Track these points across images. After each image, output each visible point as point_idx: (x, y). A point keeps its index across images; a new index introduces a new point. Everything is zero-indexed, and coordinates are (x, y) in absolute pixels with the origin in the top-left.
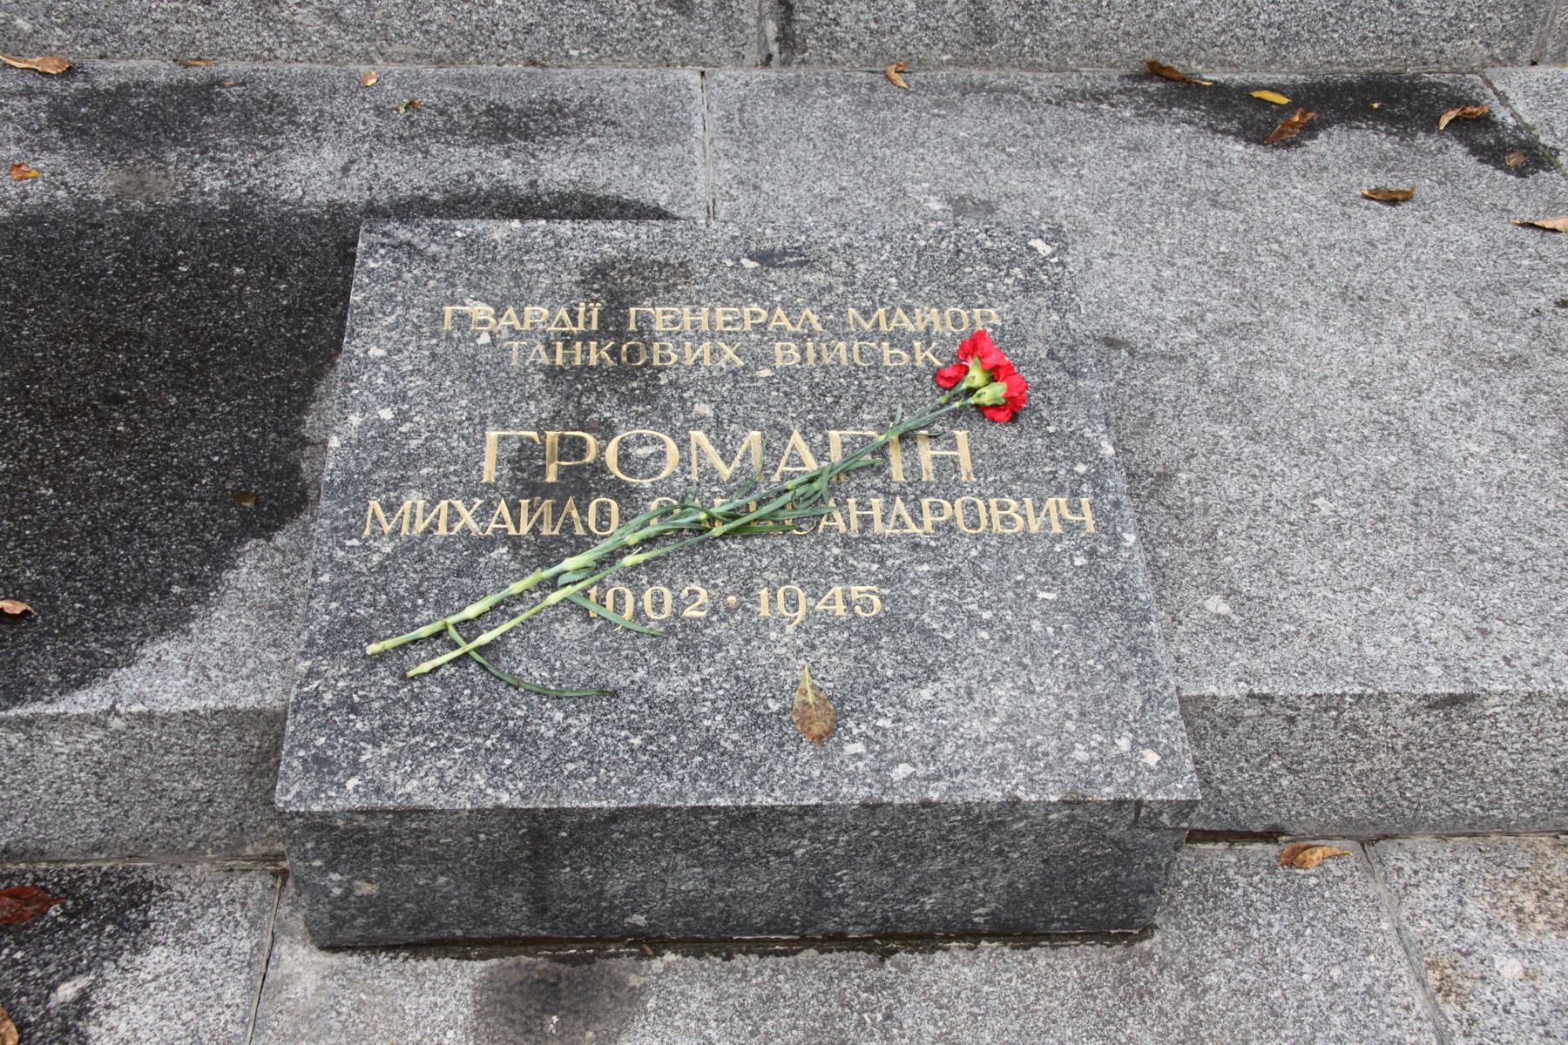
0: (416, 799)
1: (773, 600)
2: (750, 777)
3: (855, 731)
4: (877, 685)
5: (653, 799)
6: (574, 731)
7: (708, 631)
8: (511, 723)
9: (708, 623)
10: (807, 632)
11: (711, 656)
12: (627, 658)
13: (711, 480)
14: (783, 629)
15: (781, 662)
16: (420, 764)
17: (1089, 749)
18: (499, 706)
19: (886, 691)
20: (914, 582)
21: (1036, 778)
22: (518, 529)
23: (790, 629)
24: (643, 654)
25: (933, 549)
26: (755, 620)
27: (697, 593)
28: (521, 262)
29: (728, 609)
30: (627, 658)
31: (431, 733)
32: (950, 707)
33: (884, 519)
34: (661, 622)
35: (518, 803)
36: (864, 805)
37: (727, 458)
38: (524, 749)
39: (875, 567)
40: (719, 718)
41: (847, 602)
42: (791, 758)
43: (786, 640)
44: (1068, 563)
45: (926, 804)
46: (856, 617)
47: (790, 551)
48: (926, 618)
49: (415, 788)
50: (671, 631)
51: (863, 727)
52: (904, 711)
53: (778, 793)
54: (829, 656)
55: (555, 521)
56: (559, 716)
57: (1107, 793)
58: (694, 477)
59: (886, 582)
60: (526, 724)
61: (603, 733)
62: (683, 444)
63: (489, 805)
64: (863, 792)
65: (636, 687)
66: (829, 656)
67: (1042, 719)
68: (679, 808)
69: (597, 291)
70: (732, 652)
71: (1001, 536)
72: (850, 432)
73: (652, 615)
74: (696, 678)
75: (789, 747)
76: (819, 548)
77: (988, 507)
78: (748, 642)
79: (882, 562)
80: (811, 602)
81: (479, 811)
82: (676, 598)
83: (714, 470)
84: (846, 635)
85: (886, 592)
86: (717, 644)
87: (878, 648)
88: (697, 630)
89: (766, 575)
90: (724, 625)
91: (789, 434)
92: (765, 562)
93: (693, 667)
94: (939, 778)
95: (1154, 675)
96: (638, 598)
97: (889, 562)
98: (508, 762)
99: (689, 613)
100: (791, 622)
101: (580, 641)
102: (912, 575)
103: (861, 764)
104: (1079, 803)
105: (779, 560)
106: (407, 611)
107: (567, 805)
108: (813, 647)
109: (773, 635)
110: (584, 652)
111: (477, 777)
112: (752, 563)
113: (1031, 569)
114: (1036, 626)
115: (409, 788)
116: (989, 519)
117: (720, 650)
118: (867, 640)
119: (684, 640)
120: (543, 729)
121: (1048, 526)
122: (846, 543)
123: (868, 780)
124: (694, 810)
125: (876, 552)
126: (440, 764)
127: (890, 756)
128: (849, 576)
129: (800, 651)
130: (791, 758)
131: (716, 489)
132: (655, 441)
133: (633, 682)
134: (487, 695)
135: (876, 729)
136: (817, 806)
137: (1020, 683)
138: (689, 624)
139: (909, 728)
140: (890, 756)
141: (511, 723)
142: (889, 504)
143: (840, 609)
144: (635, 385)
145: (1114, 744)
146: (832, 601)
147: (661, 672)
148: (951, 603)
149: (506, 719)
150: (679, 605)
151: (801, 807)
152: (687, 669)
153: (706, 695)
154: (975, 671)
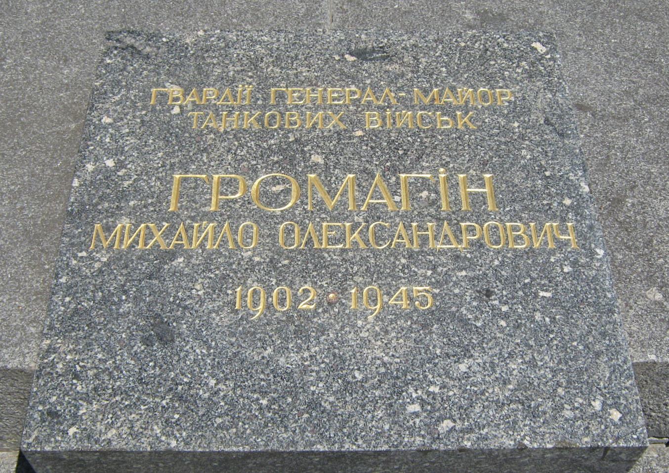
0: (114, 443)
1: (359, 298)
2: (341, 430)
3: (414, 395)
4: (430, 361)
5: (274, 446)
6: (222, 394)
7: (315, 320)
8: (180, 387)
9: (316, 313)
10: (382, 320)
11: (318, 338)
12: (260, 339)
13: (321, 209)
14: (366, 318)
15: (365, 343)
16: (118, 418)
17: (574, 409)
18: (172, 375)
19: (436, 365)
20: (456, 284)
21: (537, 430)
22: (191, 244)
23: (371, 318)
24: (270, 337)
25: (469, 260)
26: (347, 311)
27: (309, 291)
28: (203, 58)
29: (330, 304)
30: (260, 339)
31: (126, 394)
32: (479, 377)
33: (436, 238)
34: (283, 313)
35: (182, 447)
36: (419, 451)
37: (331, 193)
38: (188, 408)
39: (429, 273)
40: (321, 385)
41: (411, 299)
42: (370, 415)
43: (368, 326)
45: (463, 450)
46: (416, 310)
47: (372, 261)
49: (114, 436)
50: (290, 319)
51: (420, 392)
52: (447, 380)
53: (360, 442)
54: (398, 339)
55: (215, 239)
56: (212, 382)
57: (586, 441)
58: (309, 207)
59: (438, 284)
60: (190, 388)
61: (241, 396)
62: (303, 184)
63: (163, 448)
64: (418, 440)
65: (265, 361)
66: (398, 339)
67: (542, 386)
68: (291, 452)
69: (251, 77)
70: (331, 335)
71: (515, 250)
72: (414, 175)
73: (278, 308)
74: (306, 354)
76: (392, 259)
77: (505, 229)
78: (342, 328)
79: (434, 269)
80: (386, 298)
81: (156, 452)
82: (295, 295)
84: (409, 323)
85: (437, 291)
86: (322, 329)
87: (431, 333)
88: (308, 319)
89: (355, 278)
90: (327, 315)
91: (373, 177)
92: (356, 268)
93: (304, 346)
94: (470, 430)
95: (617, 353)
97: (439, 269)
98: (177, 416)
99: (303, 306)
100: (372, 314)
101: (229, 327)
102: (454, 279)
103: (417, 421)
104: (566, 448)
105: (365, 267)
107: (215, 449)
108: (387, 332)
109: (360, 323)
110: (233, 334)
111: (155, 427)
112: (347, 270)
113: (534, 275)
114: (538, 316)
115: (109, 435)
117: (323, 334)
118: (424, 326)
119: (298, 328)
120: (201, 392)
121: (546, 243)
122: (411, 255)
123: (422, 432)
124: (302, 453)
125: (431, 262)
126: (130, 418)
127: (437, 414)
128: (412, 279)
129: (377, 334)
130: (370, 415)
131: (323, 216)
132: (284, 181)
133: (263, 358)
134: (165, 366)
135: (429, 394)
136: (387, 451)
137: (527, 359)
138: (302, 314)
139: (451, 393)
140: (437, 414)
141: (180, 387)
142: (440, 226)
143: (404, 304)
144: (272, 142)
145: (590, 405)
147: (282, 350)
149: (177, 384)
151: (375, 452)
152: (300, 348)
153: (313, 367)
154: (497, 350)
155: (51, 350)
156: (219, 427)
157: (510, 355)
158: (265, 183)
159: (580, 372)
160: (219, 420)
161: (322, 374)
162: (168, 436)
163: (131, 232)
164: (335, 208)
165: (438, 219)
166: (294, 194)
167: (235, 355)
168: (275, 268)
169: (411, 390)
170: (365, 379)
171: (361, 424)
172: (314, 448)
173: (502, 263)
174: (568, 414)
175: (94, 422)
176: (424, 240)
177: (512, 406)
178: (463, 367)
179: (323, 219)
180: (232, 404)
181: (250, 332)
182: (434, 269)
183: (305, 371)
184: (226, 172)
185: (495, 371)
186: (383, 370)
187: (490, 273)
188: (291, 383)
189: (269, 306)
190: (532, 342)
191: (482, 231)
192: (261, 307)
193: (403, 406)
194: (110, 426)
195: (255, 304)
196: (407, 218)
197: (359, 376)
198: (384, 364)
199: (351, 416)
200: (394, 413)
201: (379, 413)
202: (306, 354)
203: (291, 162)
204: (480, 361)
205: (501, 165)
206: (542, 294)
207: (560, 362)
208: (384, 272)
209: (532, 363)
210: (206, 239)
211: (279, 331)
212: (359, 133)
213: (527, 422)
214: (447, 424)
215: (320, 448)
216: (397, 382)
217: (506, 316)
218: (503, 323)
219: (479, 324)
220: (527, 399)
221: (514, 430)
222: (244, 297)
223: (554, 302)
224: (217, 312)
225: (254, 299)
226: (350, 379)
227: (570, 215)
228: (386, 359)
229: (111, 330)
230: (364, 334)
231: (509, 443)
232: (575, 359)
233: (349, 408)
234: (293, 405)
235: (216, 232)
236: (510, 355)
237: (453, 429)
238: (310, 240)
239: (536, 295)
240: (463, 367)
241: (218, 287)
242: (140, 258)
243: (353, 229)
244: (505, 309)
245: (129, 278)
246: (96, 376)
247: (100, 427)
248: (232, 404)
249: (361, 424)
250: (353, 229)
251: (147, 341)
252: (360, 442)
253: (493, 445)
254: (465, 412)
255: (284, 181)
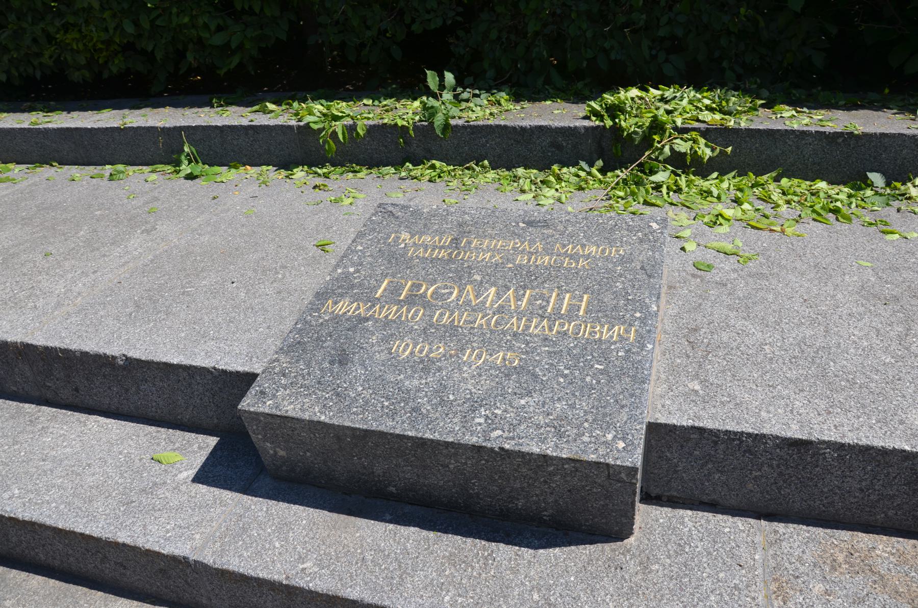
1: (470, 355)
5: (382, 428)
15: (464, 380)
20: (538, 354)
23: (474, 367)
29: (451, 355)
32: (532, 409)
33: (536, 327)
35: (327, 420)
37: (477, 297)
44: (615, 354)
46: (505, 365)
48: (537, 370)
49: (290, 409)
50: (422, 361)
59: (527, 353)
64: (475, 439)
75: (450, 416)
77: (586, 326)
80: (488, 357)
83: (471, 301)
85: (524, 357)
88: (434, 362)
94: (513, 439)
96: (415, 347)
103: (479, 428)
106: (322, 341)
108: (480, 375)
110: (383, 365)
114: (588, 379)
116: (585, 332)
118: (506, 375)
121: (612, 337)
122: (515, 335)
128: (510, 348)
135: (493, 413)
146: (497, 358)
148: (552, 364)
150: (431, 351)
151: (445, 442)
152: (421, 378)
154: (551, 395)
155: (277, 360)
156: (354, 413)
157: (559, 399)
158: (439, 288)
159: (605, 415)
160: (355, 410)
161: (429, 394)
162: (321, 413)
163: (348, 305)
164: (477, 305)
165: (542, 317)
166: (454, 295)
167: (380, 376)
168: (425, 333)
169: (483, 409)
170: (456, 400)
171: (442, 424)
172: (406, 433)
173: (576, 346)
174: (586, 439)
175: (283, 400)
176: (527, 327)
177: (548, 429)
178: (523, 402)
179: (466, 310)
180: (367, 402)
181: (394, 363)
182: (527, 344)
183: (419, 390)
184: (418, 279)
185: (544, 407)
186: (469, 396)
187: (565, 350)
188: (407, 395)
189: (412, 353)
190: (577, 394)
191: (570, 327)
192: (407, 353)
193: (473, 418)
194: (291, 403)
195: (404, 350)
196: (520, 315)
197: (452, 398)
198: (471, 393)
199: (437, 419)
200: (465, 421)
201: (455, 420)
202: (424, 381)
203: (460, 279)
204: (536, 400)
205: (599, 290)
206: (596, 366)
207: (593, 407)
208: (491, 340)
209: (572, 406)
210: (390, 314)
211: (412, 367)
212: (511, 265)
213: (554, 439)
214: (499, 432)
215: (410, 434)
216: (475, 405)
217: (565, 376)
218: (562, 380)
219: (544, 379)
220: (560, 426)
221: (543, 442)
222: (399, 346)
223: (602, 372)
224: (379, 353)
225: (404, 349)
226: (446, 399)
227: (636, 323)
228: (473, 390)
229: (314, 355)
230: (465, 375)
231: (536, 450)
232: (605, 407)
233: (438, 414)
234: (403, 408)
235: (397, 311)
236: (559, 399)
237: (501, 436)
238: (454, 320)
239: (592, 366)
240: (523, 402)
241: (386, 340)
242: (347, 320)
243: (483, 318)
244: (566, 372)
245: (335, 329)
246: (295, 377)
247: (286, 403)
248: (367, 402)
249: (442, 424)
250: (483, 318)
251: (332, 363)
252: (436, 434)
253: (525, 449)
254: (512, 427)
255: (451, 287)
